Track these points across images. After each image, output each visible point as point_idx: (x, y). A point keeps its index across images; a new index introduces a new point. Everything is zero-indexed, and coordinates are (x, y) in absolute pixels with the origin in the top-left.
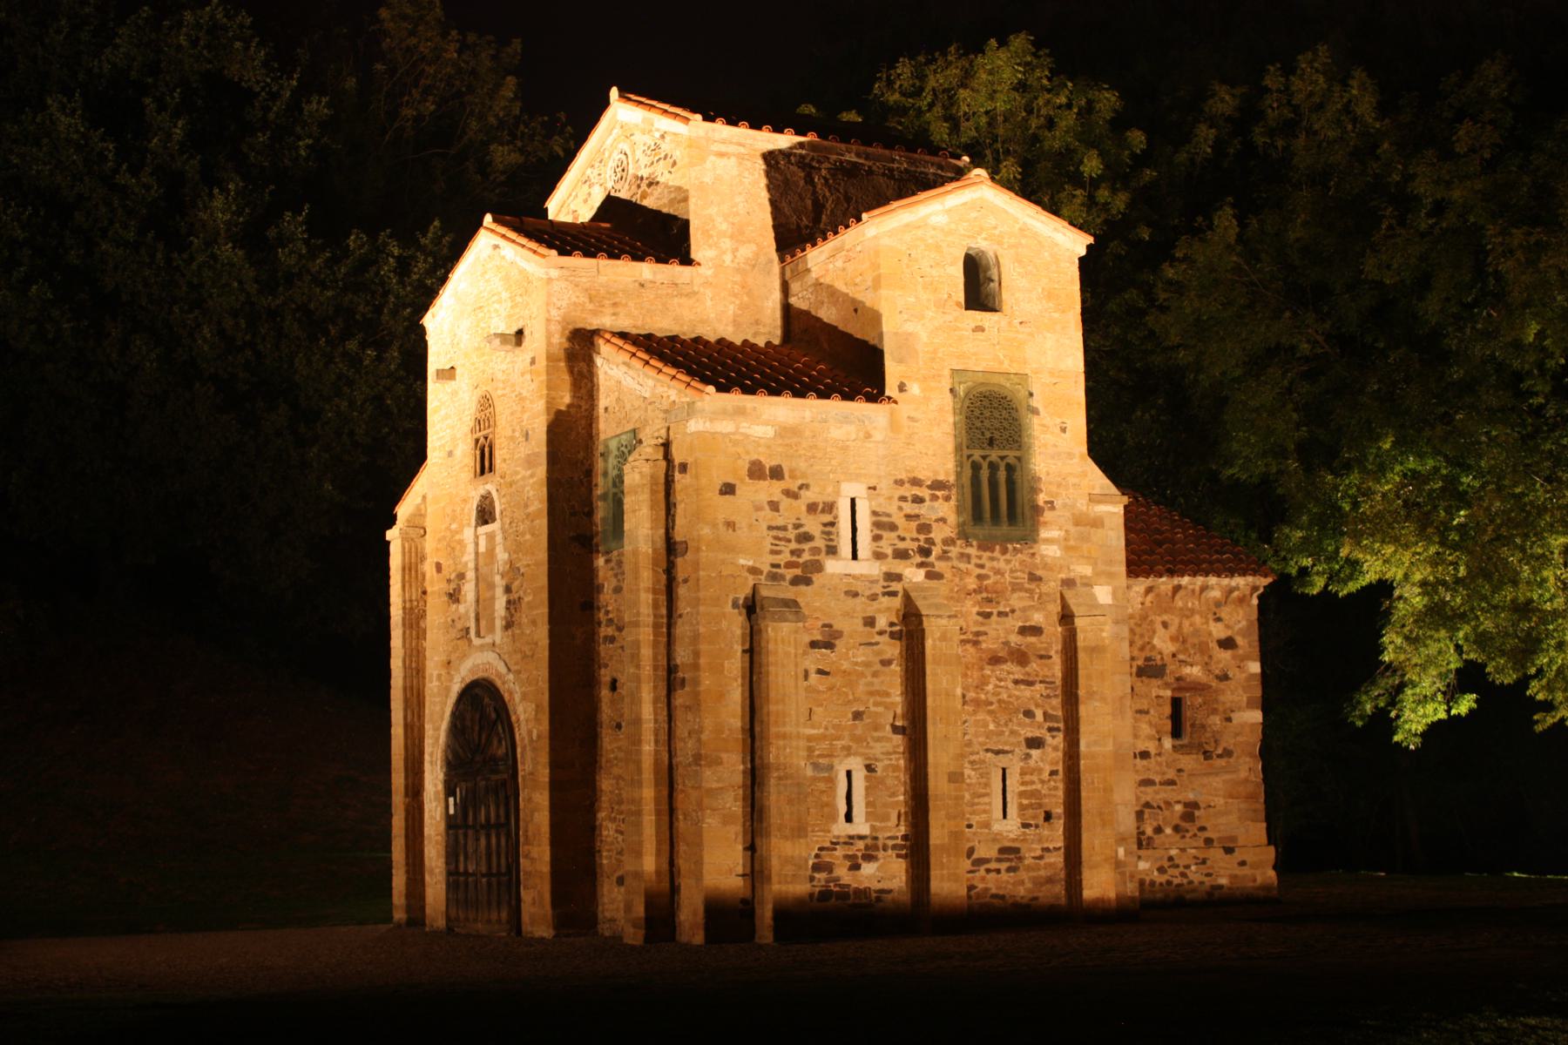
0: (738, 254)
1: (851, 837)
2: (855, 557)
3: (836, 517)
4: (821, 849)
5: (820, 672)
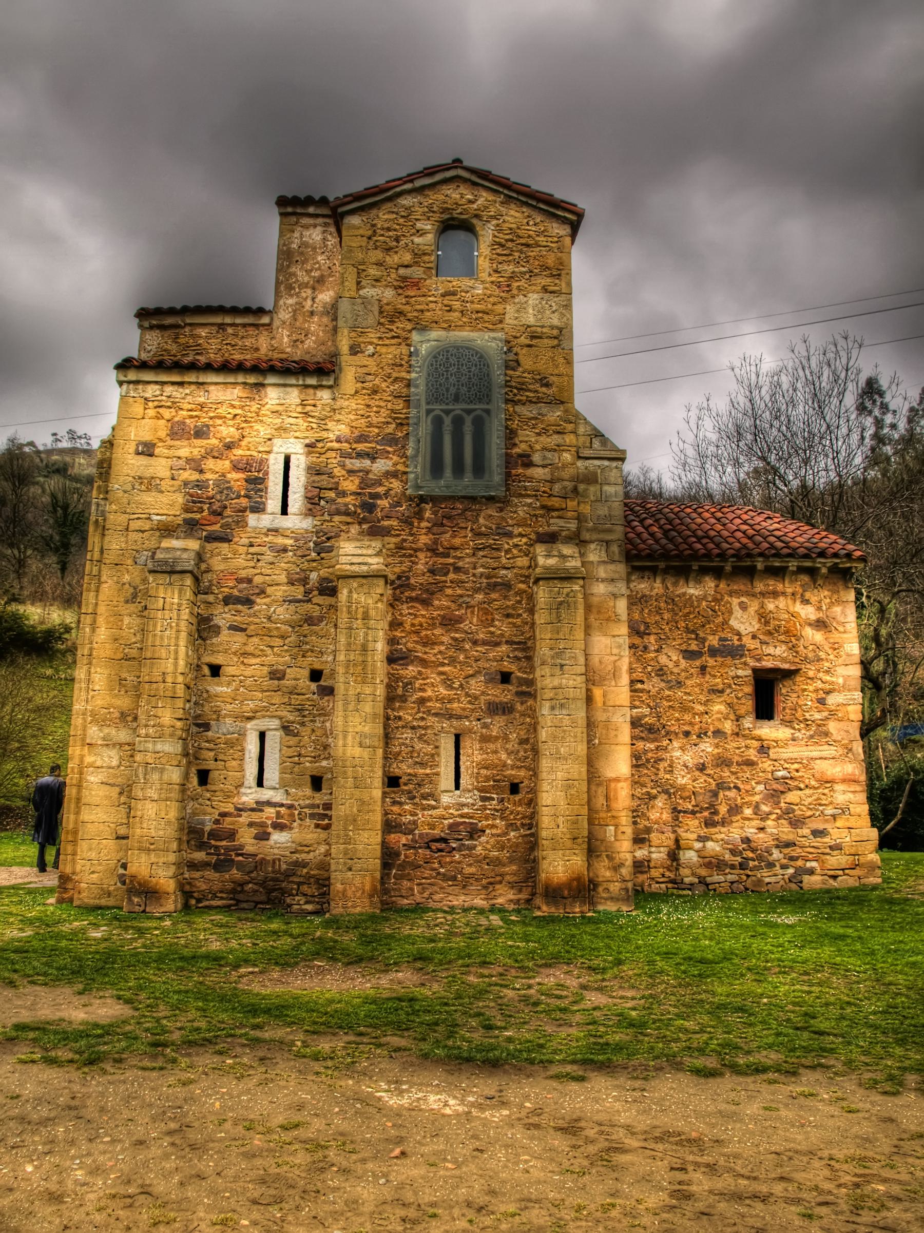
0: (317, 300)
1: (257, 803)
2: (284, 511)
3: (267, 473)
4: (224, 815)
5: (233, 628)
